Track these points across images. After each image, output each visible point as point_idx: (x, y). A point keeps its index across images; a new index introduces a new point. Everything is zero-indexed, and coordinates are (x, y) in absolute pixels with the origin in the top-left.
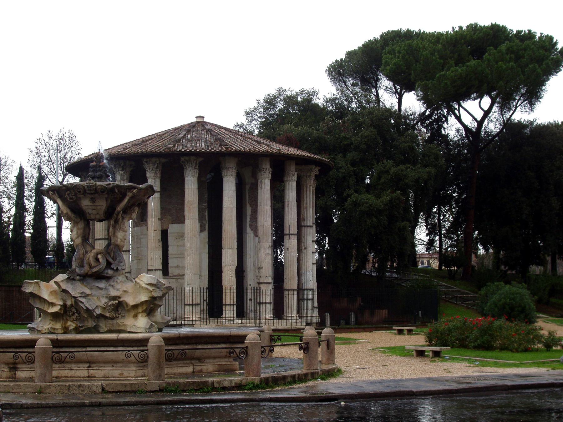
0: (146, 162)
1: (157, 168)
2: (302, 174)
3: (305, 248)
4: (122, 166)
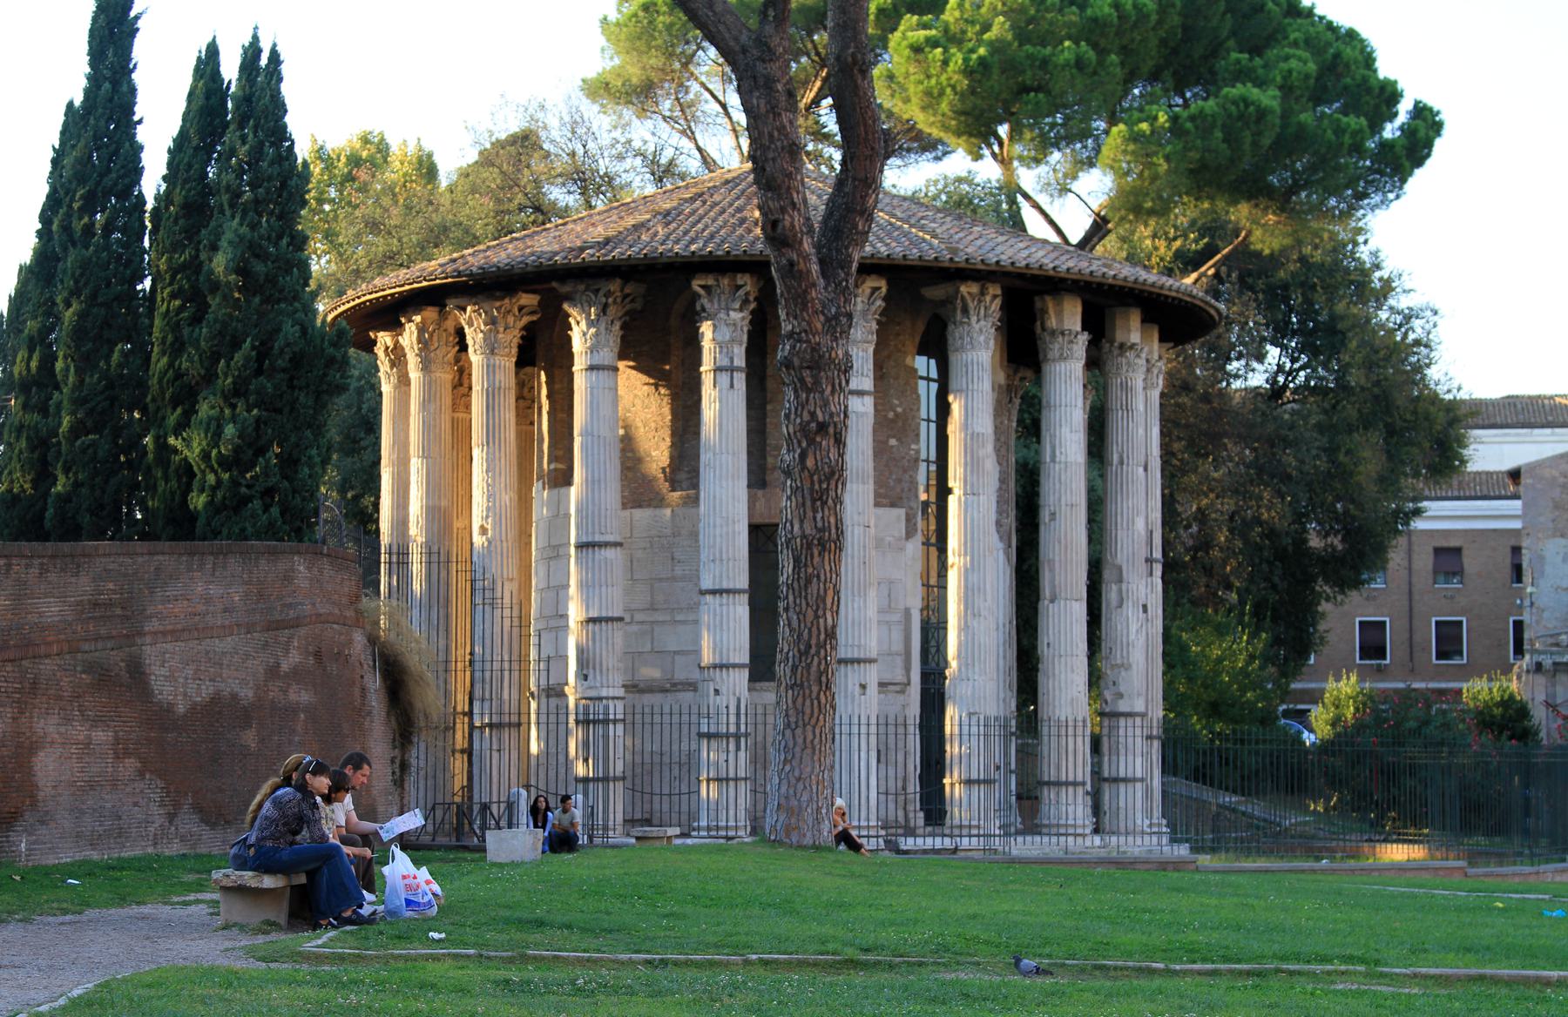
4: (741, 292)
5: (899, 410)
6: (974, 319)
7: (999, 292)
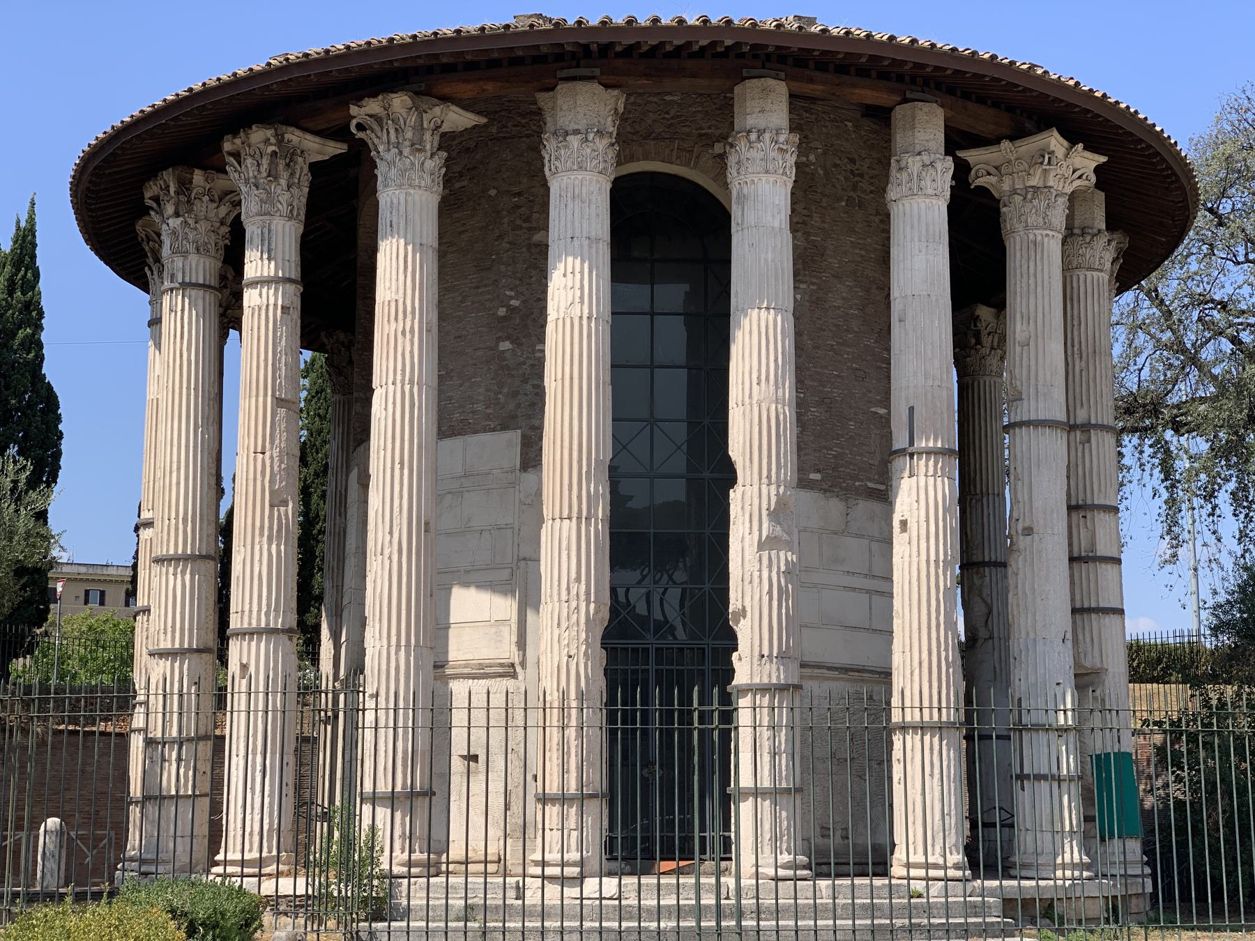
0: (237, 155)
1: (273, 175)
2: (1006, 187)
3: (1029, 531)
5: (514, 303)
6: (381, 148)
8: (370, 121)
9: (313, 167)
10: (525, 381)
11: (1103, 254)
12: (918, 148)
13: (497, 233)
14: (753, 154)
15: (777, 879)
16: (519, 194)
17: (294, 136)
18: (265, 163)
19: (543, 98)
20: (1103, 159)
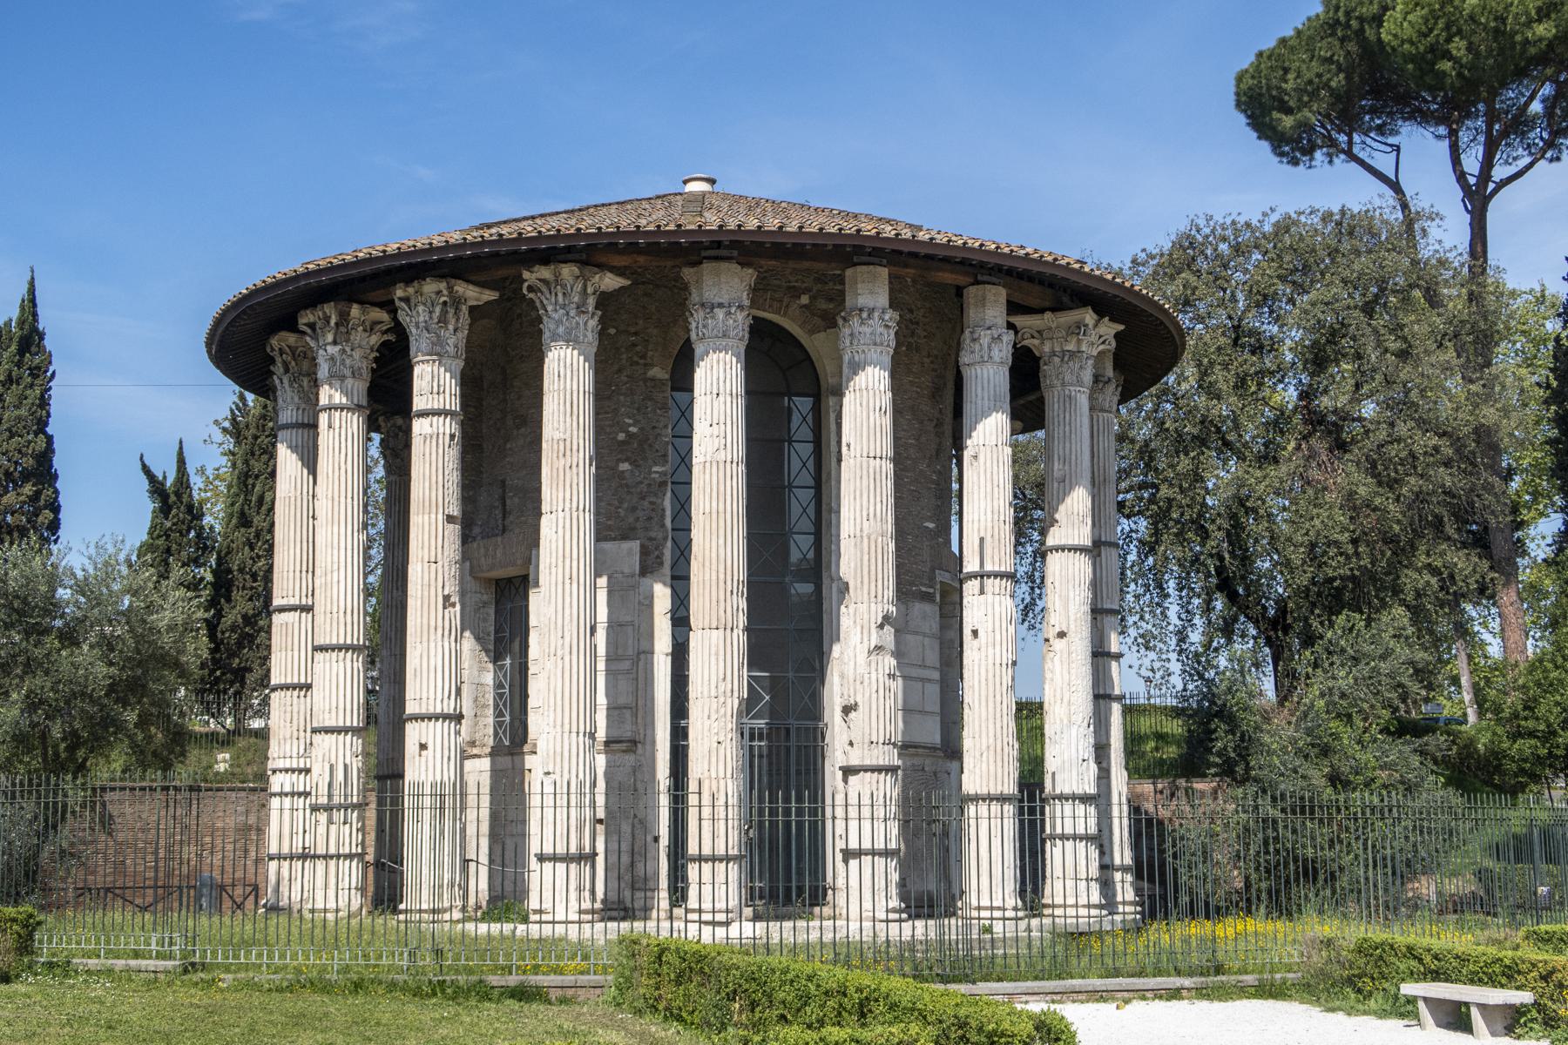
0: (406, 300)
1: (443, 320)
2: (1047, 348)
6: (550, 308)
7: (576, 270)
8: (539, 284)
9: (472, 309)
10: (643, 498)
11: (1111, 394)
12: (988, 323)
13: (616, 367)
14: (865, 329)
15: (887, 921)
16: (636, 334)
17: (461, 288)
18: (438, 309)
19: (687, 273)
20: (1122, 327)
